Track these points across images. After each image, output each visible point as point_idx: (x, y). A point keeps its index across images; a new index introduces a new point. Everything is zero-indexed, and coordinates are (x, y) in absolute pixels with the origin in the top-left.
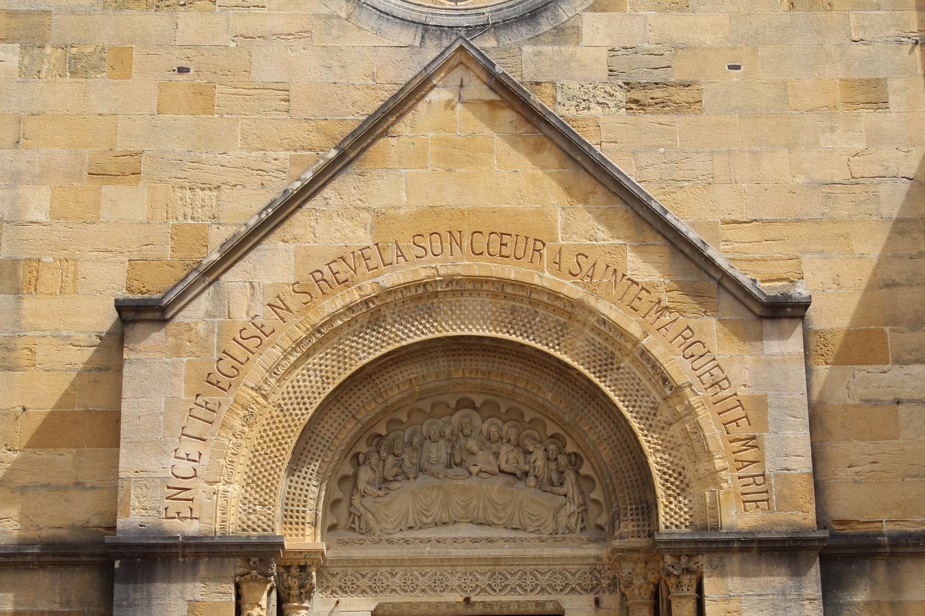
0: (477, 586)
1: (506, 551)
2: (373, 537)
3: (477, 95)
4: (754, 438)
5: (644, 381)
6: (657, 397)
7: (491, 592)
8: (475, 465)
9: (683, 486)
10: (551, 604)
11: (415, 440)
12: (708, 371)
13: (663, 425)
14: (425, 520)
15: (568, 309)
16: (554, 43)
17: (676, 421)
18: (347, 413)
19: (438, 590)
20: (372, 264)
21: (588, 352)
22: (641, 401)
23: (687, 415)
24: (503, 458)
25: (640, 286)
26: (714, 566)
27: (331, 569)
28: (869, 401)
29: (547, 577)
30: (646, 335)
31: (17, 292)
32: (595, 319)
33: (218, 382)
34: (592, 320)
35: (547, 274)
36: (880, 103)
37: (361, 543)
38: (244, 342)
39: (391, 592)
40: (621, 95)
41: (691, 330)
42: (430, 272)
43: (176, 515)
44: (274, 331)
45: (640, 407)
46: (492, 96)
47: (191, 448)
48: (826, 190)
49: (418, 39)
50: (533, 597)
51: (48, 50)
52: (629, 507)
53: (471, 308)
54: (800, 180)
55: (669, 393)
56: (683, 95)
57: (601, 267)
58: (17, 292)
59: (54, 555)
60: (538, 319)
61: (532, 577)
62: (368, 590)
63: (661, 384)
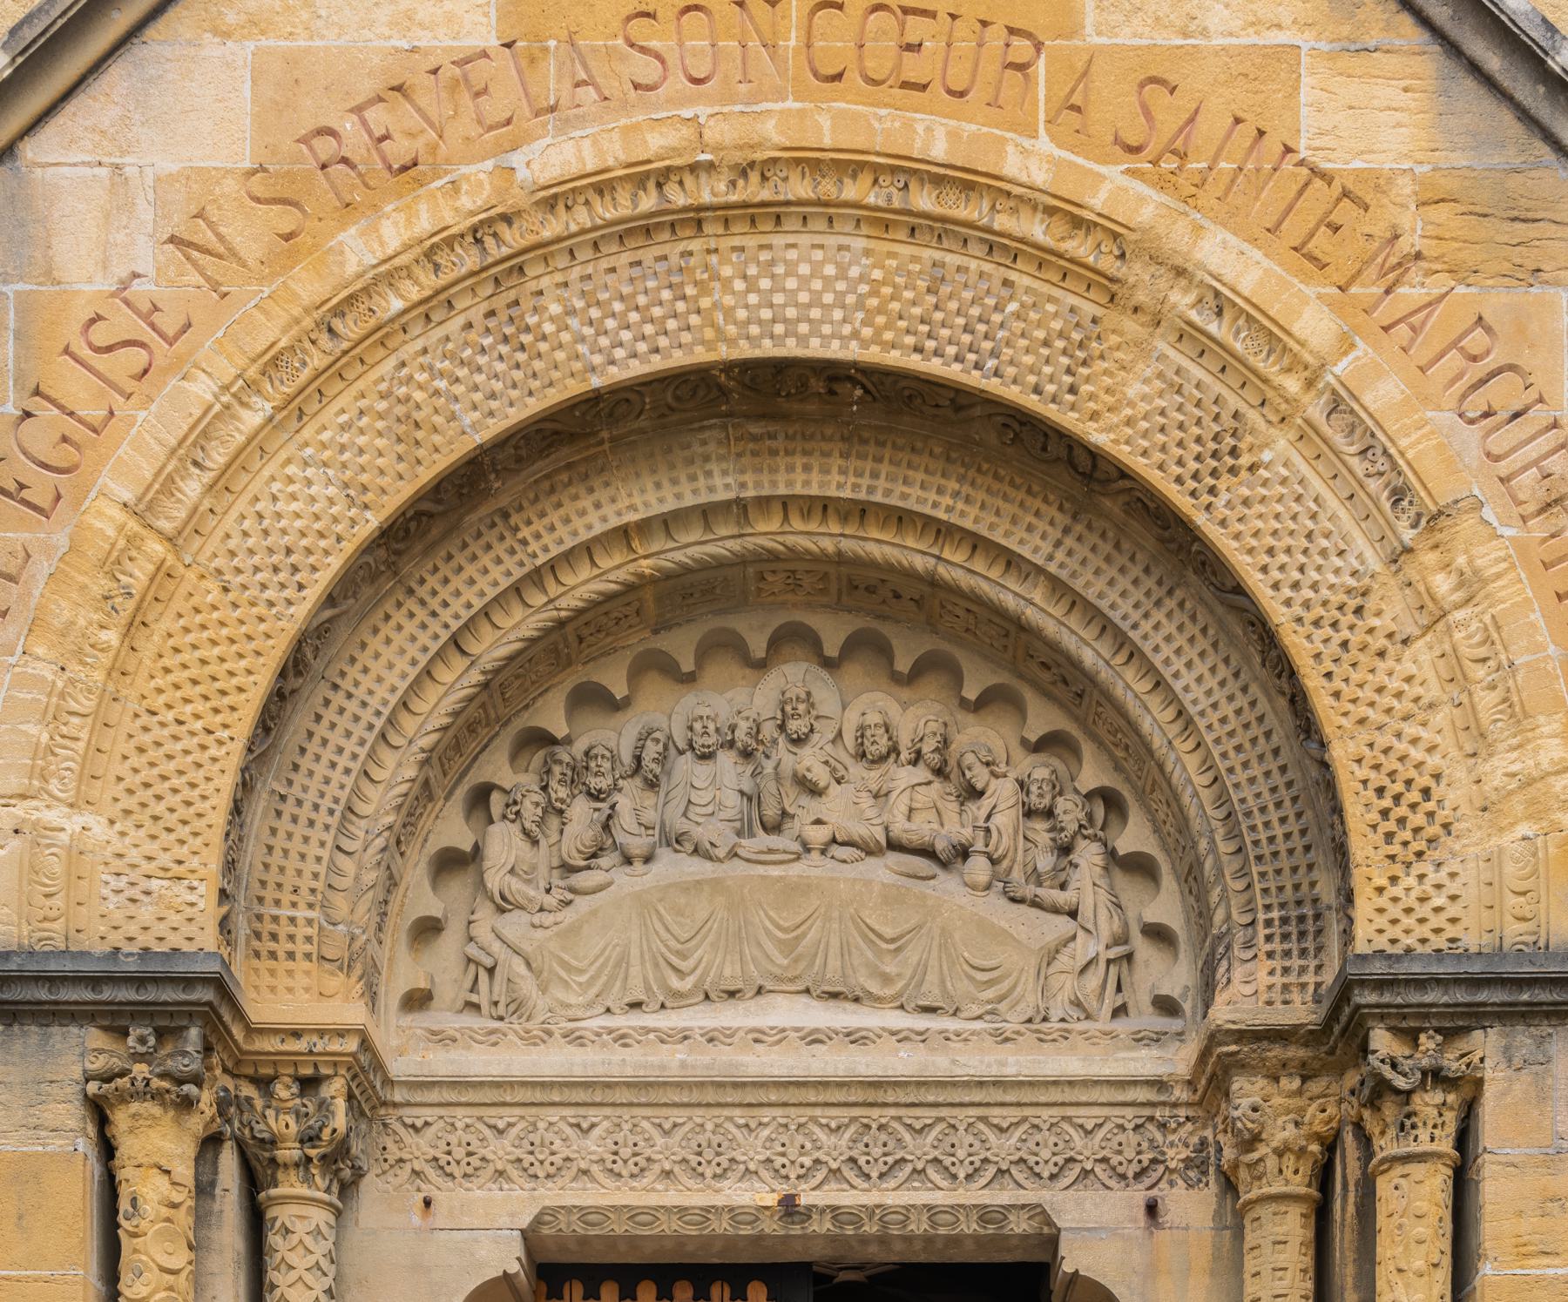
1: (902, 1062)
2: (529, 1025)
6: (1369, 554)
9: (1434, 830)
10: (1024, 1215)
13: (1380, 642)
17: (1427, 629)
18: (435, 626)
21: (1163, 413)
22: (1319, 568)
23: (1458, 607)
29: (1013, 1141)
30: (1346, 345)
32: (1191, 298)
45: (1314, 587)
52: (1261, 916)
53: (804, 269)
55: (1408, 535)
60: (1012, 307)
61: (970, 1139)
63: (1387, 506)
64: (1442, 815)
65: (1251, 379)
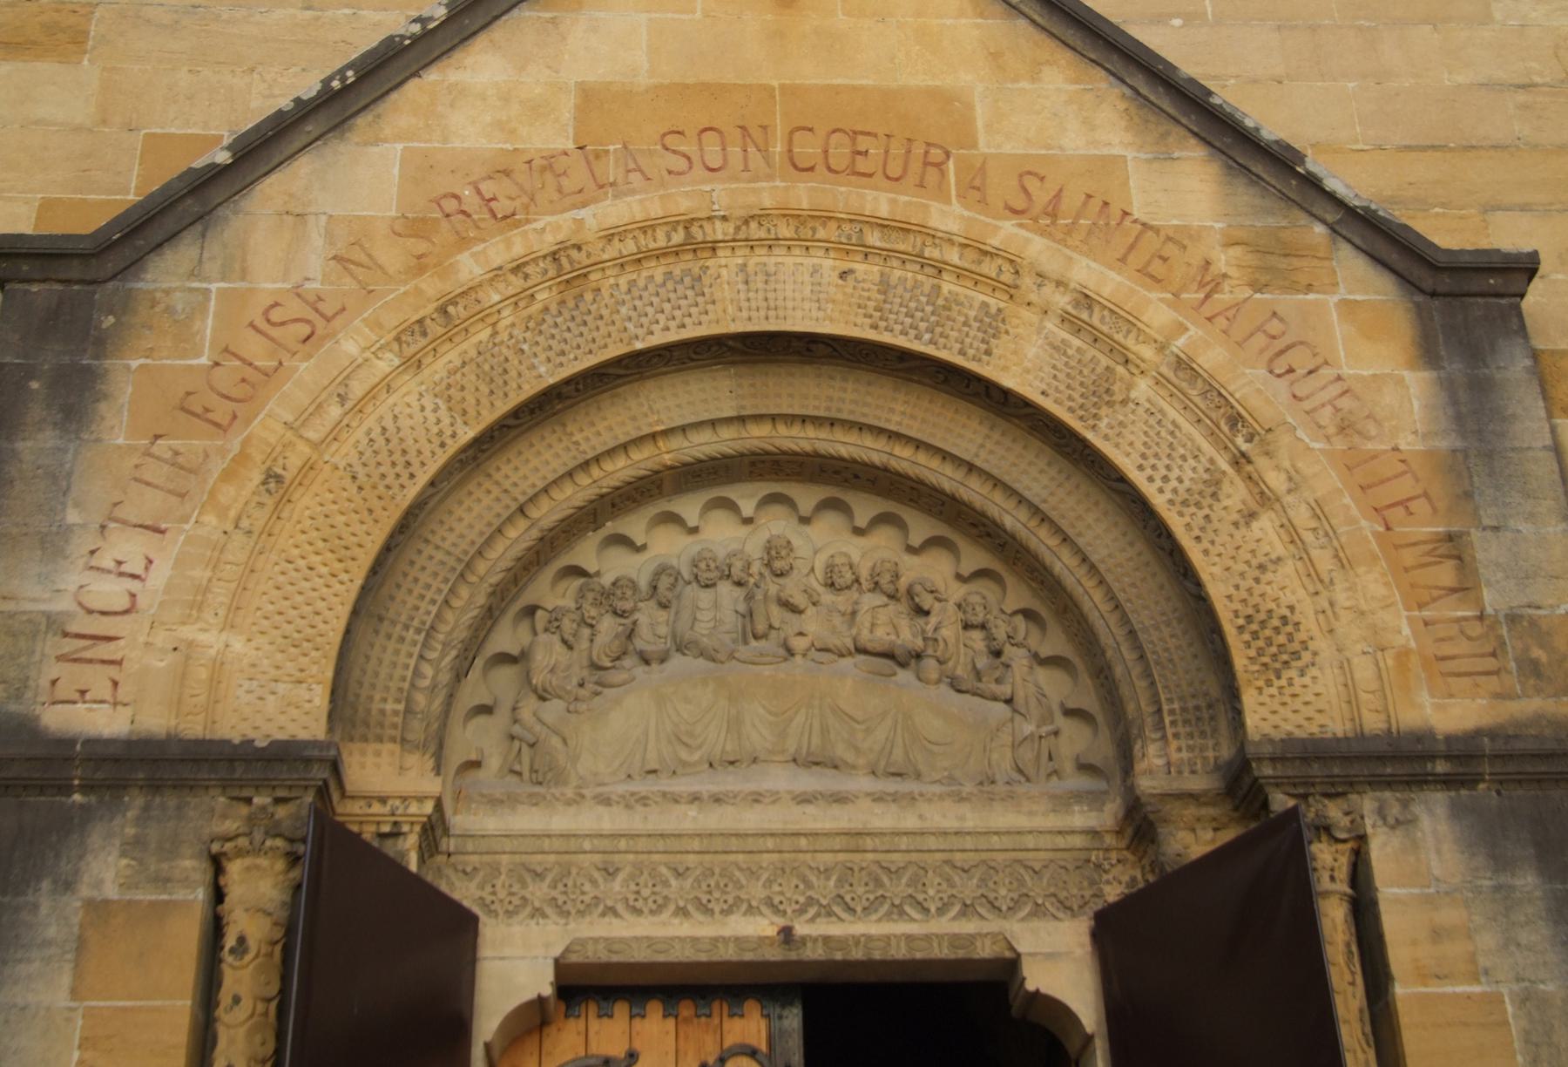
0: (810, 898)
5: (1186, 426)
7: (844, 915)
8: (801, 634)
11: (665, 582)
12: (1330, 402)
13: (1235, 517)
14: (684, 754)
15: (1007, 277)
19: (717, 910)
24: (864, 619)
25: (1162, 233)
26: (1391, 820)
27: (461, 858)
32: (1067, 298)
33: (207, 410)
37: (535, 801)
38: (275, 332)
39: (603, 915)
41: (1281, 320)
43: (76, 696)
44: (344, 309)
50: (945, 925)
54: (1461, 79)
57: (1071, 201)
62: (549, 910)
63: (1225, 428)
64: (1302, 636)
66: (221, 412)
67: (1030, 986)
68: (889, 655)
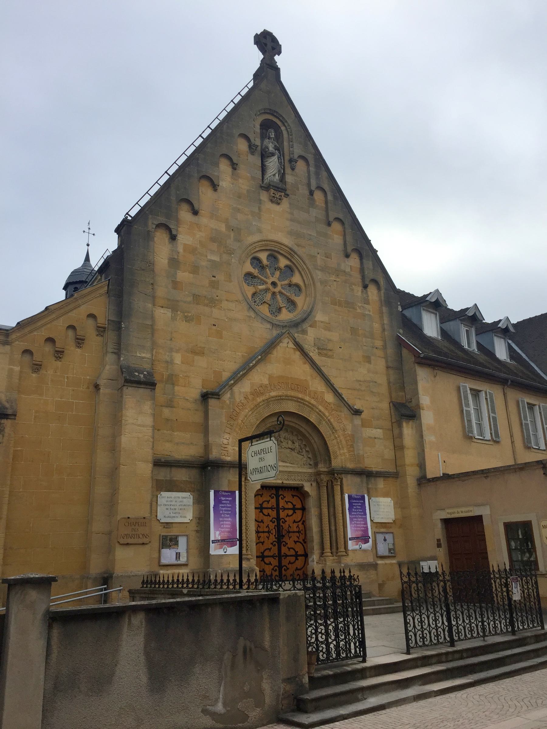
3: (291, 346)
4: (352, 445)
16: (302, 334)
20: (268, 389)
28: (369, 437)
31: (173, 384)
34: (317, 410)
35: (308, 397)
36: (369, 362)
38: (239, 407)
40: (317, 350)
42: (282, 393)
46: (295, 348)
47: (227, 436)
48: (360, 383)
49: (271, 327)
51: (179, 313)
54: (354, 379)
56: (330, 353)
58: (173, 384)
59: (187, 464)
65: (322, 417)
66: (234, 418)
67: (305, 490)
68: (291, 449)
